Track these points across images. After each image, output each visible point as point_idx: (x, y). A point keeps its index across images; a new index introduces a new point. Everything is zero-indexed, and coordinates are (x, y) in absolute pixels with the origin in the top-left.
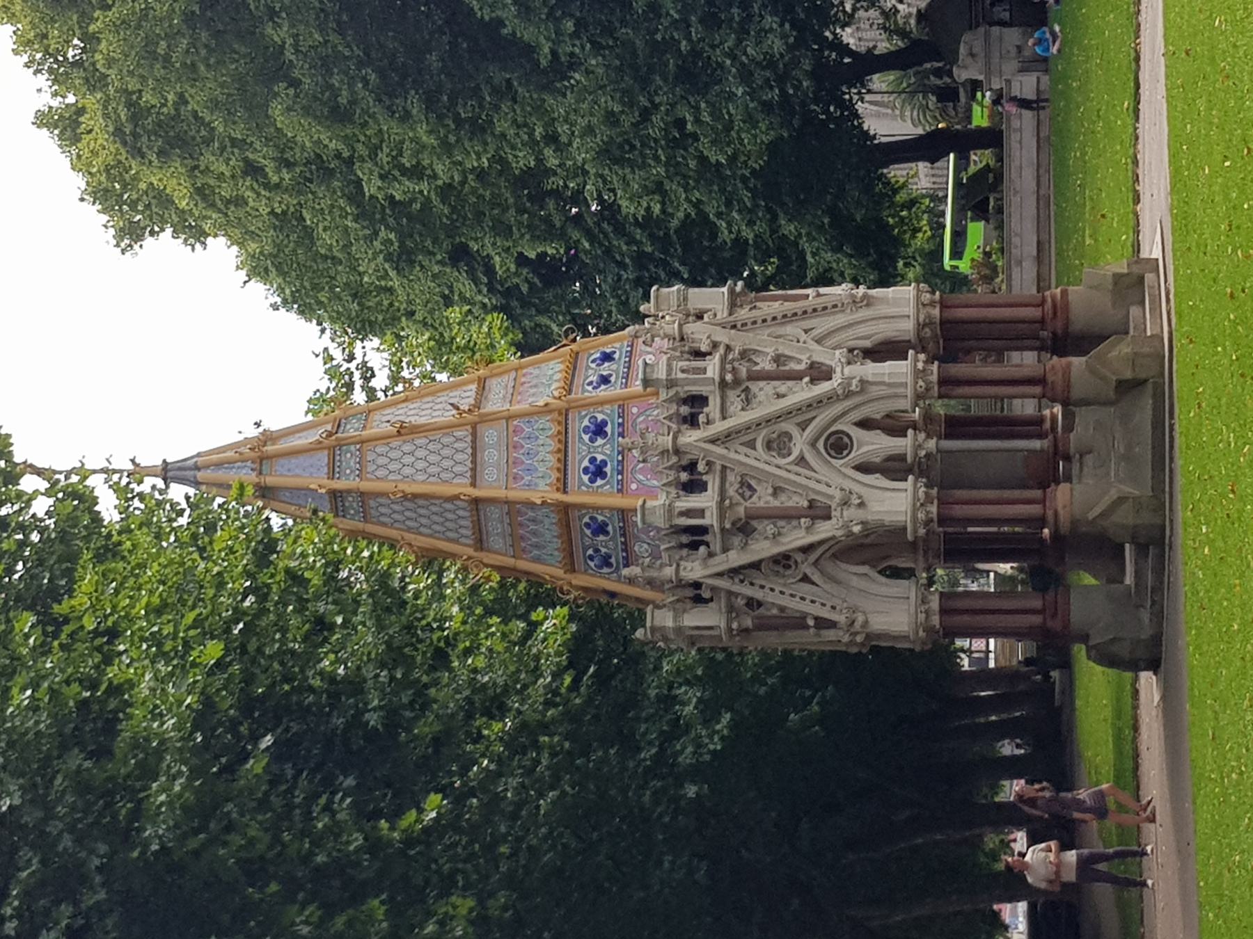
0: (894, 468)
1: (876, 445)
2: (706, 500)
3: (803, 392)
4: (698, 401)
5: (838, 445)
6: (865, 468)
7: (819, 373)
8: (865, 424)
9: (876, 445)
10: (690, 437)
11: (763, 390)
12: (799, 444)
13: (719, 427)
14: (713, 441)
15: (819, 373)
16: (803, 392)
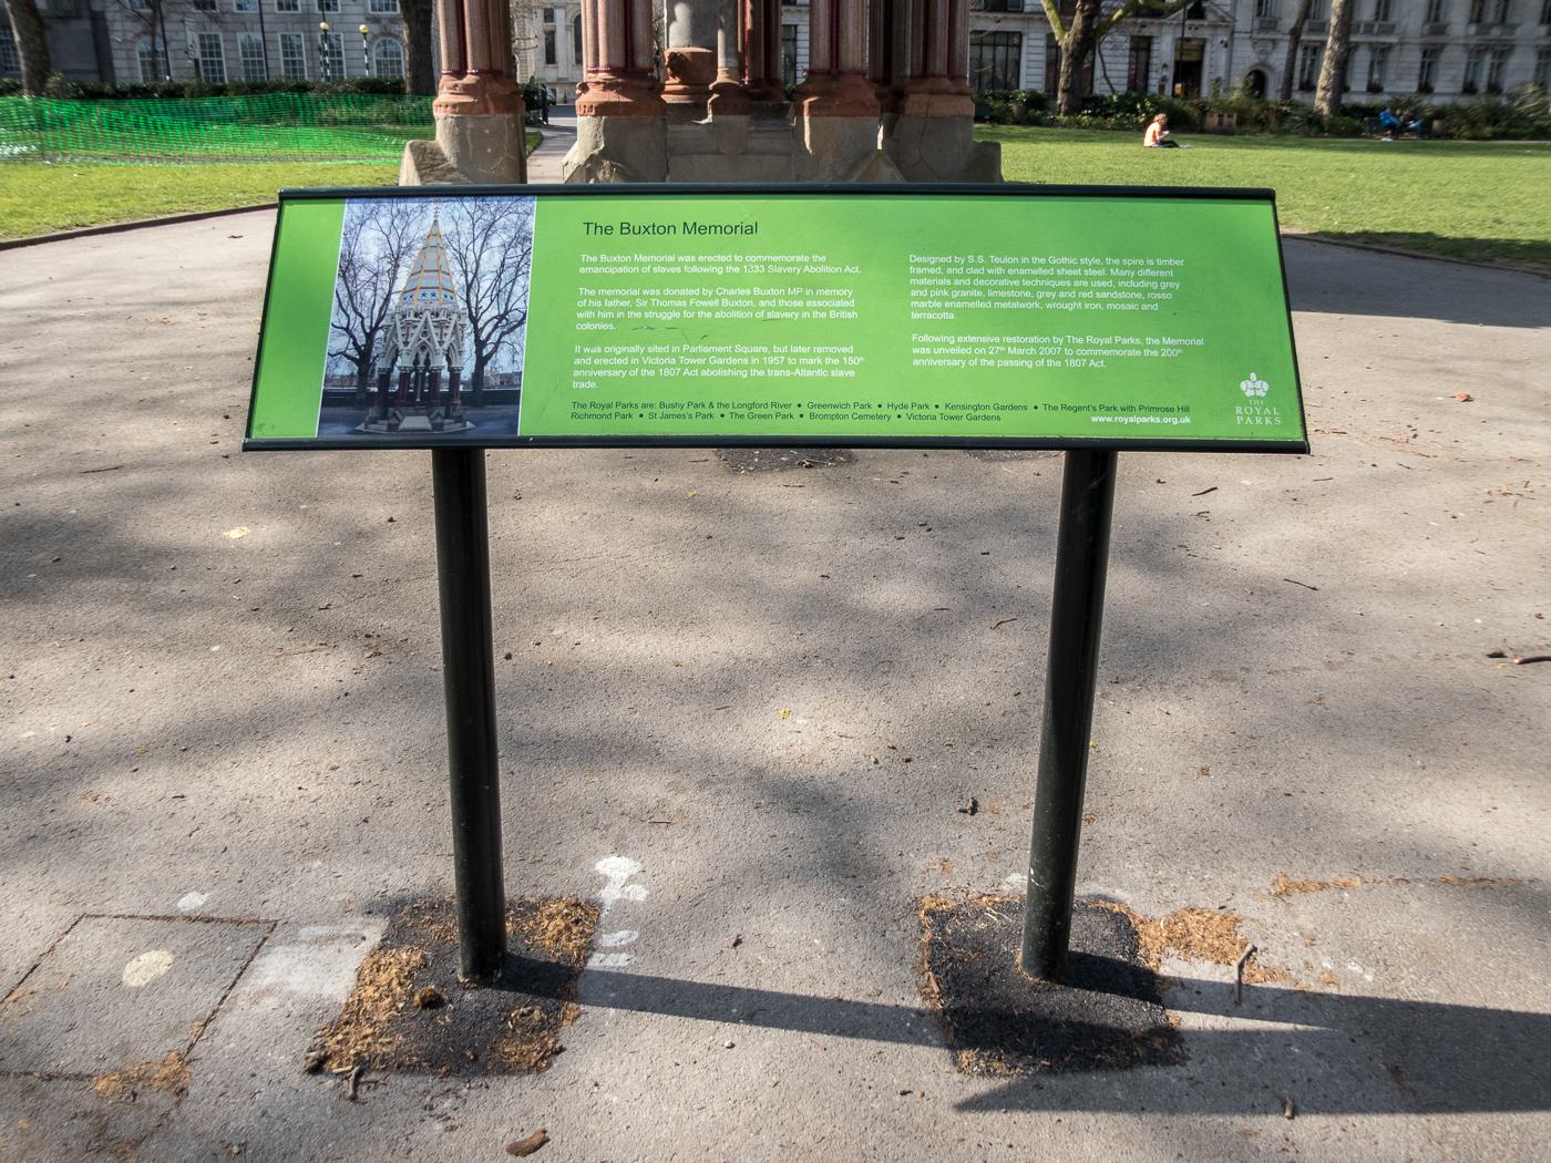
0: (416, 362)
1: (422, 357)
2: (412, 318)
3: (436, 339)
4: (437, 315)
5: (423, 347)
6: (417, 355)
7: (441, 343)
8: (428, 355)
9: (422, 357)
10: (427, 314)
11: (438, 331)
12: (424, 339)
13: (430, 320)
14: (426, 322)
15: (441, 343)
16: (436, 339)
